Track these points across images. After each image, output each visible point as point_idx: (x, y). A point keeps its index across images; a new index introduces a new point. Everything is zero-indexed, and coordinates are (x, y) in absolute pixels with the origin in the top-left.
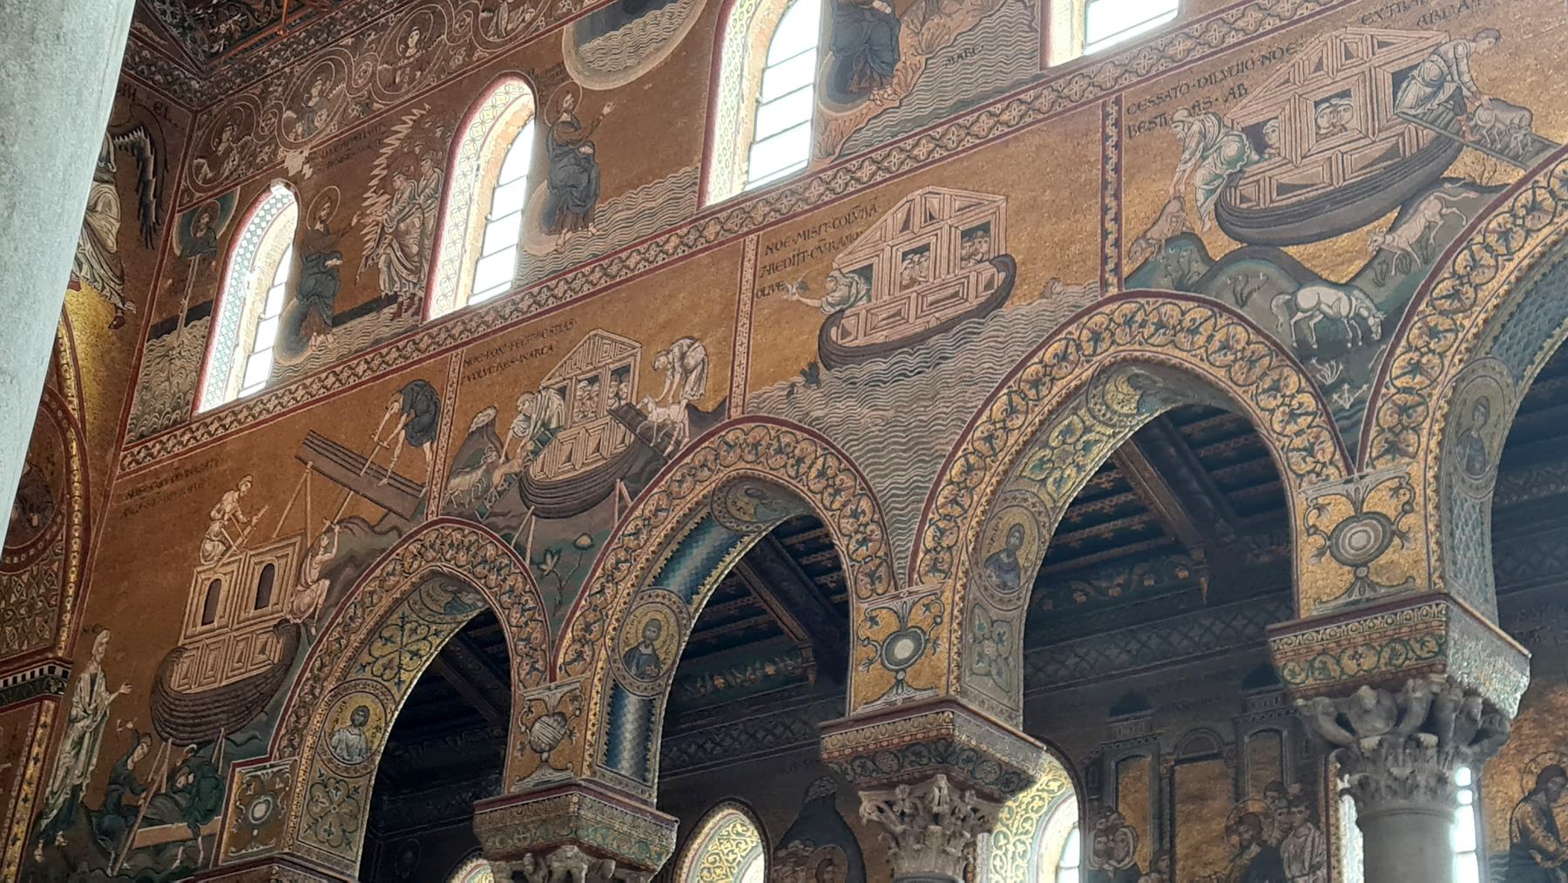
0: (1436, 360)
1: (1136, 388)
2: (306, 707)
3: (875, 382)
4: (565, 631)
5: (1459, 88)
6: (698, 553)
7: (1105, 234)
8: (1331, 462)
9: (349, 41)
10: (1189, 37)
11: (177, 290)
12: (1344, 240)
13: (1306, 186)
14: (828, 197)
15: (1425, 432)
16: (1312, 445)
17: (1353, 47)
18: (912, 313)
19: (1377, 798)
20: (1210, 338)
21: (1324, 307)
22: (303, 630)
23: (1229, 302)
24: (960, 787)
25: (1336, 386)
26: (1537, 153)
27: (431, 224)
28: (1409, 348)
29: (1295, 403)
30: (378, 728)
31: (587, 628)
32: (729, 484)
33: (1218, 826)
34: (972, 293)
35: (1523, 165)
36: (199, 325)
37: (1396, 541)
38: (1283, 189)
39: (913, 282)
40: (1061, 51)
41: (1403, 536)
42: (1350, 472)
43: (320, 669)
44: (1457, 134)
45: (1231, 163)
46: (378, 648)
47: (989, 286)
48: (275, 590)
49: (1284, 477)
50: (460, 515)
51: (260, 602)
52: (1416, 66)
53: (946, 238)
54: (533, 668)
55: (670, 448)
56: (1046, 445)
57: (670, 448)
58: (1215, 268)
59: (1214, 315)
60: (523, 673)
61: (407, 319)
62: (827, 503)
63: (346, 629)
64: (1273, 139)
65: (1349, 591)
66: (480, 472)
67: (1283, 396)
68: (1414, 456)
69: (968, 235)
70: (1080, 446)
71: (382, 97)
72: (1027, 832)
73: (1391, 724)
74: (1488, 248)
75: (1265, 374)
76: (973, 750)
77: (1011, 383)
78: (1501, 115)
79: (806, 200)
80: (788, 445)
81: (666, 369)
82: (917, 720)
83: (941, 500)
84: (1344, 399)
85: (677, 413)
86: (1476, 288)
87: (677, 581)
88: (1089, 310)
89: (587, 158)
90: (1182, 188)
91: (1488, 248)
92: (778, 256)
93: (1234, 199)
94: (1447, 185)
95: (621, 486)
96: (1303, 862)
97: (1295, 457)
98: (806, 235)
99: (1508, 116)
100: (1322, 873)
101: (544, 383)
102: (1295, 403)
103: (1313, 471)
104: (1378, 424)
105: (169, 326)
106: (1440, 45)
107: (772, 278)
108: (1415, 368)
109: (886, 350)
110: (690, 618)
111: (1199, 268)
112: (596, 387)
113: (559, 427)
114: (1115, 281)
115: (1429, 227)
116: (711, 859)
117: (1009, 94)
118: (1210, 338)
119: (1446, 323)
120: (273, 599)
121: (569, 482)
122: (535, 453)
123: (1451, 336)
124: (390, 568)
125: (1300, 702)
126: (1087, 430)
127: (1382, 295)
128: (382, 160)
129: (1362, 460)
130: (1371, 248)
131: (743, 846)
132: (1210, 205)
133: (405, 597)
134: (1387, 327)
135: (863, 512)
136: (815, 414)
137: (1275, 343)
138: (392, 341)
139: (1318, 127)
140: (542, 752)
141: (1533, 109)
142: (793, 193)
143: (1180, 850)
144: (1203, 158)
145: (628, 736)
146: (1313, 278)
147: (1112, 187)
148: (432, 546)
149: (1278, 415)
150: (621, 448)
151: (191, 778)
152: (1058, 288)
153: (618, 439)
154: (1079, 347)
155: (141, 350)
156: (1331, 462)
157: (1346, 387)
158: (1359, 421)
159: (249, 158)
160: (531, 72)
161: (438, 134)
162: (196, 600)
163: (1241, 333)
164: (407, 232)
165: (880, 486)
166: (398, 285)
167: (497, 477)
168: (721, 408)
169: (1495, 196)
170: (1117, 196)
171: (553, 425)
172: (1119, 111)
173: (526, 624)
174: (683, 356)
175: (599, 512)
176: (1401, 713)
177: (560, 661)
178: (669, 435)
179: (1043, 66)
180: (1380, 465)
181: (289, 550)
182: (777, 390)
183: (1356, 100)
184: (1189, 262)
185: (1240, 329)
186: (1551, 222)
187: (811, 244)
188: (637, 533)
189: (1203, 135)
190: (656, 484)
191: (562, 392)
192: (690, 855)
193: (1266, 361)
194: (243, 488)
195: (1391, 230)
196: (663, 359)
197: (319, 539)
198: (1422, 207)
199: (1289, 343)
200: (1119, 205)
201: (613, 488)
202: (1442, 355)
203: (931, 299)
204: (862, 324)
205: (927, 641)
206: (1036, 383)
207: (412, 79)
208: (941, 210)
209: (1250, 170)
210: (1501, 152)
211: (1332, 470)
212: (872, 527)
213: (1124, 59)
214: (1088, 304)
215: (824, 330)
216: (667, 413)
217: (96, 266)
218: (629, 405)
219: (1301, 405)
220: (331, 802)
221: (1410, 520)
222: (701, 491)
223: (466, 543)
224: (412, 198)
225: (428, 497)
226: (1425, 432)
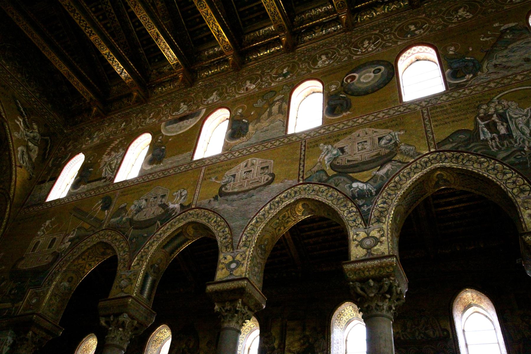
0: (390, 201)
1: (303, 208)
2: (56, 274)
3: (233, 200)
4: (136, 257)
5: (396, 142)
6: (177, 242)
7: (300, 169)
8: (361, 224)
9: (107, 124)
10: (325, 129)
11: (48, 174)
12: (365, 173)
13: (354, 161)
14: (226, 159)
15: (387, 218)
16: (355, 219)
17: (368, 132)
18: (245, 185)
19: (372, 311)
20: (327, 194)
21: (359, 187)
22: (60, 254)
23: (333, 186)
24: (244, 304)
25: (363, 205)
26: (418, 155)
27: (119, 162)
28: (383, 198)
29: (351, 209)
30: (75, 284)
31: (142, 257)
32: (189, 223)
33: (297, 337)
34: (262, 181)
35: (414, 158)
36: (51, 182)
37: (379, 243)
38: (348, 161)
39: (246, 178)
40: (290, 131)
41: (381, 242)
42: (366, 226)
43: (62, 265)
44: (396, 151)
45: (335, 155)
46: (80, 261)
47: (267, 180)
48: (55, 244)
49: (347, 227)
50: (112, 227)
51: (50, 247)
52: (384, 137)
53: (256, 169)
54: (124, 266)
55: (174, 214)
56: (278, 219)
57: (174, 214)
58: (329, 178)
59: (328, 189)
60: (121, 268)
61: (108, 182)
62: (216, 229)
63: (73, 255)
64: (346, 150)
65: (366, 255)
66: (119, 218)
67: (347, 208)
68: (384, 223)
69: (263, 168)
70: (286, 221)
71: (113, 135)
72: (243, 338)
73: (377, 291)
74: (404, 176)
75: (342, 202)
76: (250, 294)
77: (271, 202)
78: (407, 148)
79: (220, 160)
80: (206, 215)
81: (176, 195)
82: (236, 282)
83: (248, 229)
84: (365, 209)
85: (177, 206)
86: (401, 185)
87: (168, 249)
88: (294, 186)
89: (163, 149)
90: (321, 160)
91: (404, 176)
92: (210, 172)
93: (335, 163)
94: (393, 162)
95: (159, 222)
96: (320, 348)
97: (350, 222)
98: (218, 167)
99: (409, 148)
100: (325, 352)
101: (142, 198)
102: (351, 209)
103: (355, 226)
104: (374, 215)
105: (43, 182)
106: (390, 132)
107: (209, 176)
108: (384, 203)
109: (237, 193)
110: (170, 260)
111: (325, 178)
112: (156, 199)
113: (144, 208)
114: (302, 180)
115: (388, 170)
116: (156, 338)
117: (277, 139)
118: (327, 194)
119: (393, 193)
120: (54, 246)
121: (144, 221)
122: (136, 214)
123: (394, 196)
124: (89, 240)
125: (351, 283)
126: (289, 217)
127: (375, 185)
128: (109, 149)
129: (369, 224)
130: (372, 175)
131: (165, 336)
132: (329, 164)
133: (91, 248)
134: (377, 192)
135: (226, 231)
136: (215, 207)
137: (345, 195)
138: (103, 187)
139: (358, 148)
140: (122, 288)
141: (416, 146)
142: (216, 158)
143: (287, 343)
144: (327, 154)
145: (148, 288)
146: (357, 181)
147: (302, 160)
148: (102, 235)
149: (346, 212)
150: (160, 213)
151: (16, 291)
152: (286, 181)
153: (160, 211)
154: (291, 195)
155: (34, 187)
156: (361, 224)
157: (365, 206)
158: (369, 214)
159: (75, 147)
160: (152, 131)
161: (125, 143)
162: (32, 246)
163: (336, 193)
164: (112, 164)
165: (232, 225)
166: (107, 175)
167: (124, 219)
168: (190, 205)
169: (406, 165)
170: (304, 161)
171: (143, 207)
172: (305, 144)
173: (125, 255)
174: (181, 193)
175: (150, 229)
176: (381, 287)
177: (133, 265)
178: (174, 211)
179: (286, 133)
180: (374, 225)
181: (61, 235)
182: (206, 201)
183: (368, 143)
184: (323, 176)
185: (335, 192)
186: (421, 171)
187: (220, 169)
188: (160, 234)
189: (327, 149)
190: (168, 223)
191: (146, 200)
192: (151, 336)
193: (343, 199)
194: (53, 219)
195: (379, 170)
196: (175, 193)
197: (71, 232)
198: (387, 166)
199: (350, 195)
200: (304, 163)
201: (156, 222)
202: (392, 200)
203: (251, 182)
204: (231, 187)
205: (240, 264)
206: (278, 202)
207: (121, 132)
208: (256, 163)
209: (340, 157)
210: (408, 155)
211: (361, 226)
212: (228, 235)
213: (307, 133)
214: (294, 185)
215: (221, 188)
216: (174, 205)
217: (28, 164)
218: (164, 204)
219: (352, 210)
220: (56, 301)
221: (384, 238)
222: (181, 225)
223: (112, 235)
224: (115, 156)
225: (104, 223)
226: (387, 218)
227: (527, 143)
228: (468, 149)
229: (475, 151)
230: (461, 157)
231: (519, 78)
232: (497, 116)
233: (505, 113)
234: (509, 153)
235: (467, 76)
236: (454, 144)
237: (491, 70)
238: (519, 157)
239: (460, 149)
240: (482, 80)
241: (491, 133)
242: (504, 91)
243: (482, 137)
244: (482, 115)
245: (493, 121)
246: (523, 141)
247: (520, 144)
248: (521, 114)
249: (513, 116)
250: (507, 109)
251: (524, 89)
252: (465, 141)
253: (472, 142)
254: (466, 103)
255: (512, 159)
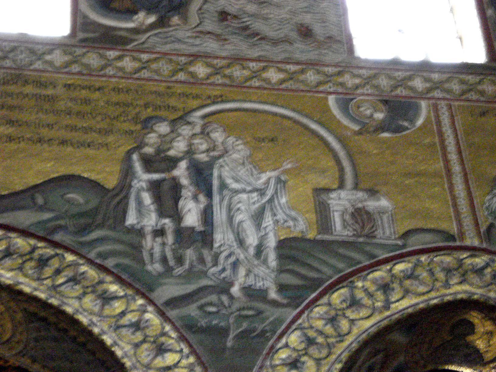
227: (242, 272)
228: (82, 244)
229: (100, 255)
230: (55, 263)
231: (273, 75)
232: (188, 168)
233: (210, 165)
234: (191, 288)
235: (141, 15)
236: (47, 216)
237: (209, 26)
238: (212, 309)
239: (58, 237)
240: (177, 46)
241: (161, 214)
242: (222, 102)
243: (131, 219)
244: (149, 150)
245: (174, 179)
246: (235, 265)
247: (224, 270)
248: (249, 184)
249: (229, 181)
250: (220, 157)
251: (275, 114)
252: (81, 215)
253: (101, 226)
254: (115, 98)
255: (192, 310)
